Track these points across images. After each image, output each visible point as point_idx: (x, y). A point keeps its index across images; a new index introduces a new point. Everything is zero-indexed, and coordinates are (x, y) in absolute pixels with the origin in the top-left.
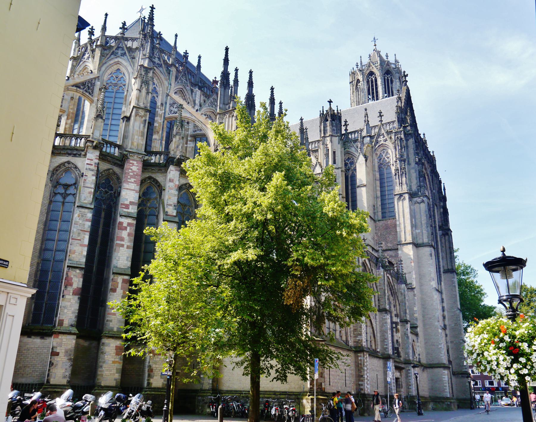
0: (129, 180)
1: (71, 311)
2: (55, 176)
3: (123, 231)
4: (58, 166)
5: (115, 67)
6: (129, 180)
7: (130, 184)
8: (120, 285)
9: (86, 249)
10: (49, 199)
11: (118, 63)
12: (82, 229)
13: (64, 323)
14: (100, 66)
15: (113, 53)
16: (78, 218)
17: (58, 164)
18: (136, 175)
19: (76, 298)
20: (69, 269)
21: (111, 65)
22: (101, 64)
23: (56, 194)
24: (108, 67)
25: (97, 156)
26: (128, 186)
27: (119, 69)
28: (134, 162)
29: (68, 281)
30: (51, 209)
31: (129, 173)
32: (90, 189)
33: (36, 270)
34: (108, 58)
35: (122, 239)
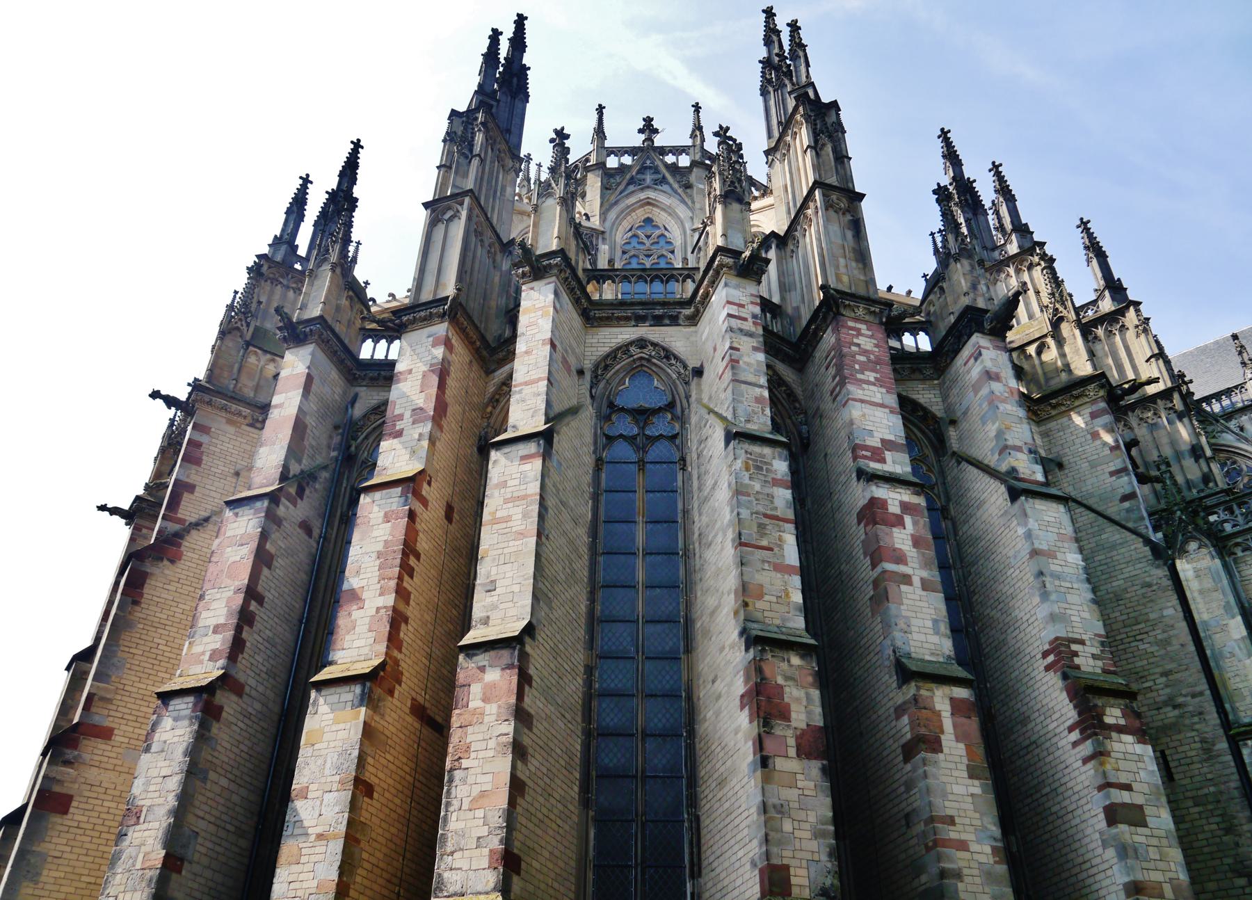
0: (859, 376)
1: (807, 826)
2: (602, 385)
3: (894, 530)
4: (608, 356)
5: (641, 214)
6: (859, 376)
7: (865, 386)
8: (948, 723)
9: (796, 581)
10: (594, 452)
11: (648, 203)
12: (769, 512)
13: (794, 880)
14: (604, 209)
15: (632, 181)
16: (747, 475)
17: (607, 349)
18: (877, 363)
19: (815, 767)
20: (763, 651)
21: (628, 207)
22: (606, 206)
23: (610, 439)
24: (622, 212)
25: (752, 295)
26: (861, 392)
27: (648, 221)
28: (859, 326)
29: (769, 698)
30: (603, 485)
31: (854, 356)
32: (758, 390)
33: (584, 693)
34: (621, 193)
35: (900, 559)
